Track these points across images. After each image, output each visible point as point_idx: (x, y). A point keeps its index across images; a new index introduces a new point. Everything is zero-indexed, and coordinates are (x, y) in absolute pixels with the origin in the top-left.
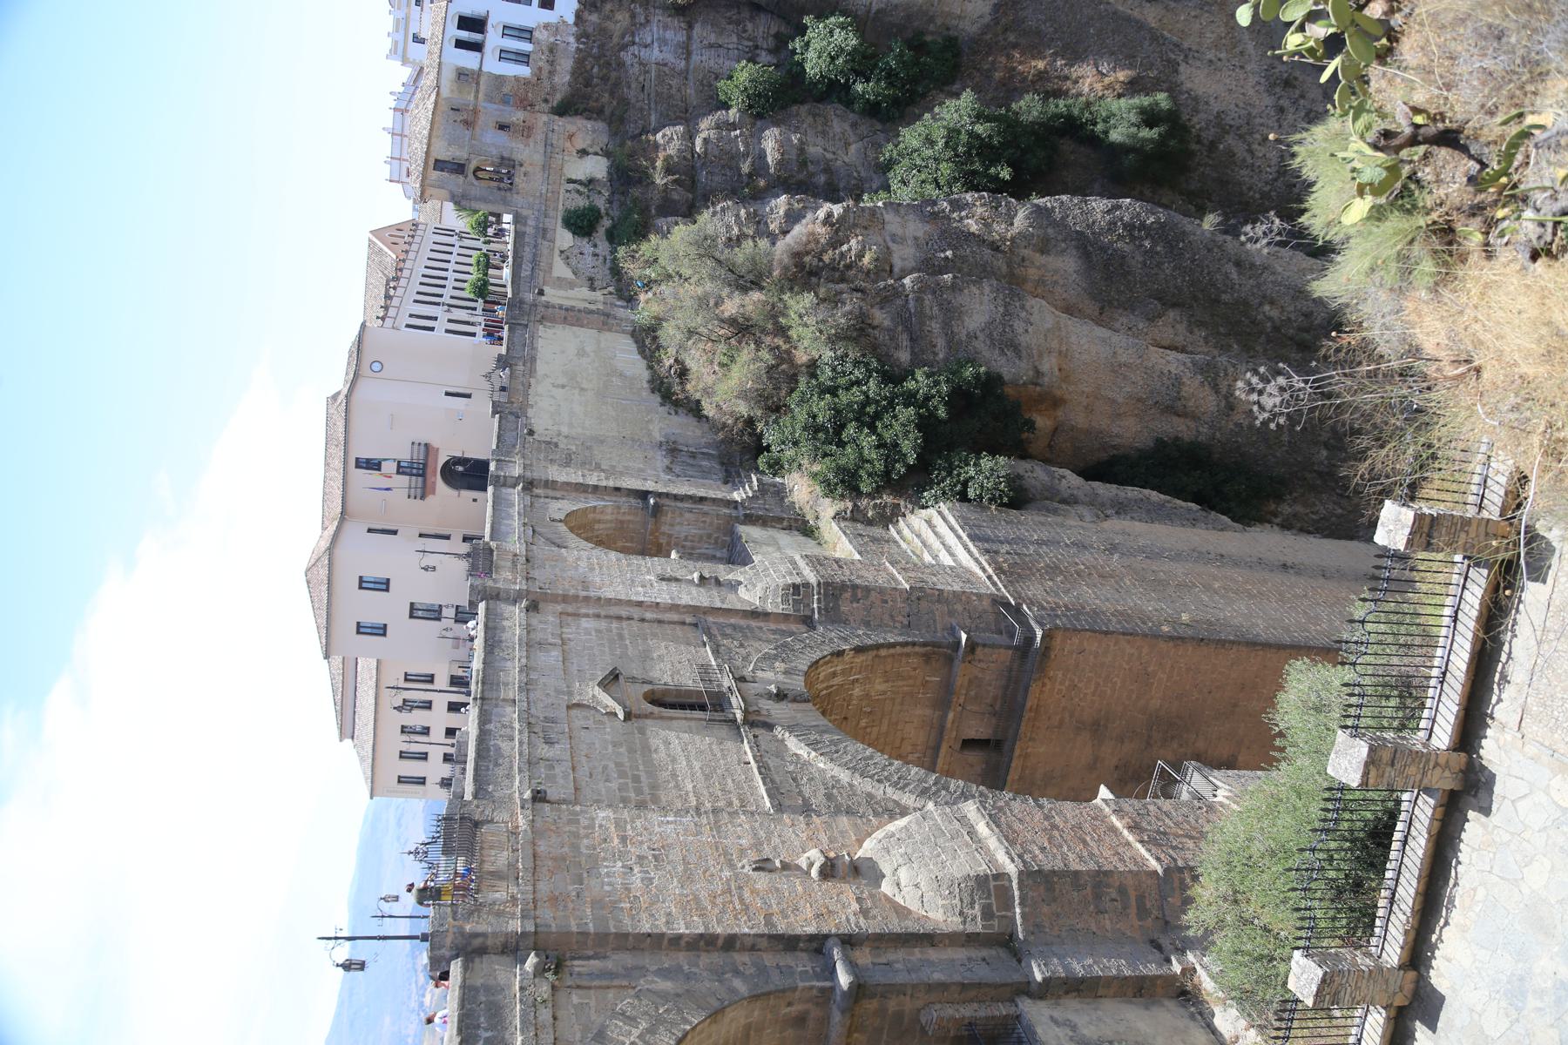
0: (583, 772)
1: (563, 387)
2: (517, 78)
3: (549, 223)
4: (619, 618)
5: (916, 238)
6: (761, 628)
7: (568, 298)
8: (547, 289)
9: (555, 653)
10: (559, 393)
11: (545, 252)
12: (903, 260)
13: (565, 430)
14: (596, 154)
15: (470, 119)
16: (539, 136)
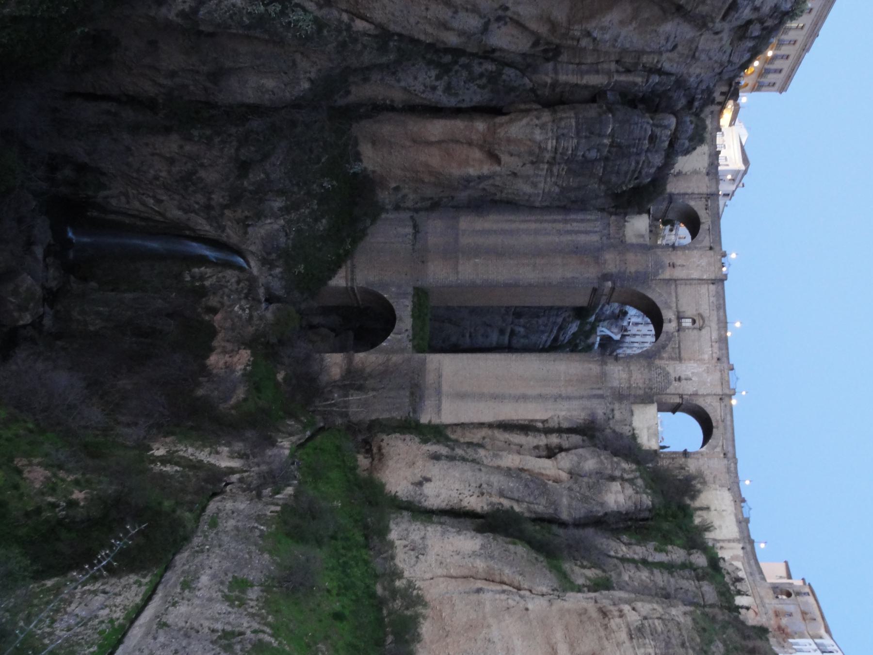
0: (707, 294)
1: (723, 511)
2: (794, 638)
3: (751, 578)
4: (699, 360)
5: (611, 493)
6: (667, 360)
7: (732, 548)
8: (740, 553)
9: (713, 338)
10: (724, 508)
11: (748, 568)
12: (617, 486)
13: (718, 492)
14: (742, 607)
15: (805, 615)
16: (771, 613)
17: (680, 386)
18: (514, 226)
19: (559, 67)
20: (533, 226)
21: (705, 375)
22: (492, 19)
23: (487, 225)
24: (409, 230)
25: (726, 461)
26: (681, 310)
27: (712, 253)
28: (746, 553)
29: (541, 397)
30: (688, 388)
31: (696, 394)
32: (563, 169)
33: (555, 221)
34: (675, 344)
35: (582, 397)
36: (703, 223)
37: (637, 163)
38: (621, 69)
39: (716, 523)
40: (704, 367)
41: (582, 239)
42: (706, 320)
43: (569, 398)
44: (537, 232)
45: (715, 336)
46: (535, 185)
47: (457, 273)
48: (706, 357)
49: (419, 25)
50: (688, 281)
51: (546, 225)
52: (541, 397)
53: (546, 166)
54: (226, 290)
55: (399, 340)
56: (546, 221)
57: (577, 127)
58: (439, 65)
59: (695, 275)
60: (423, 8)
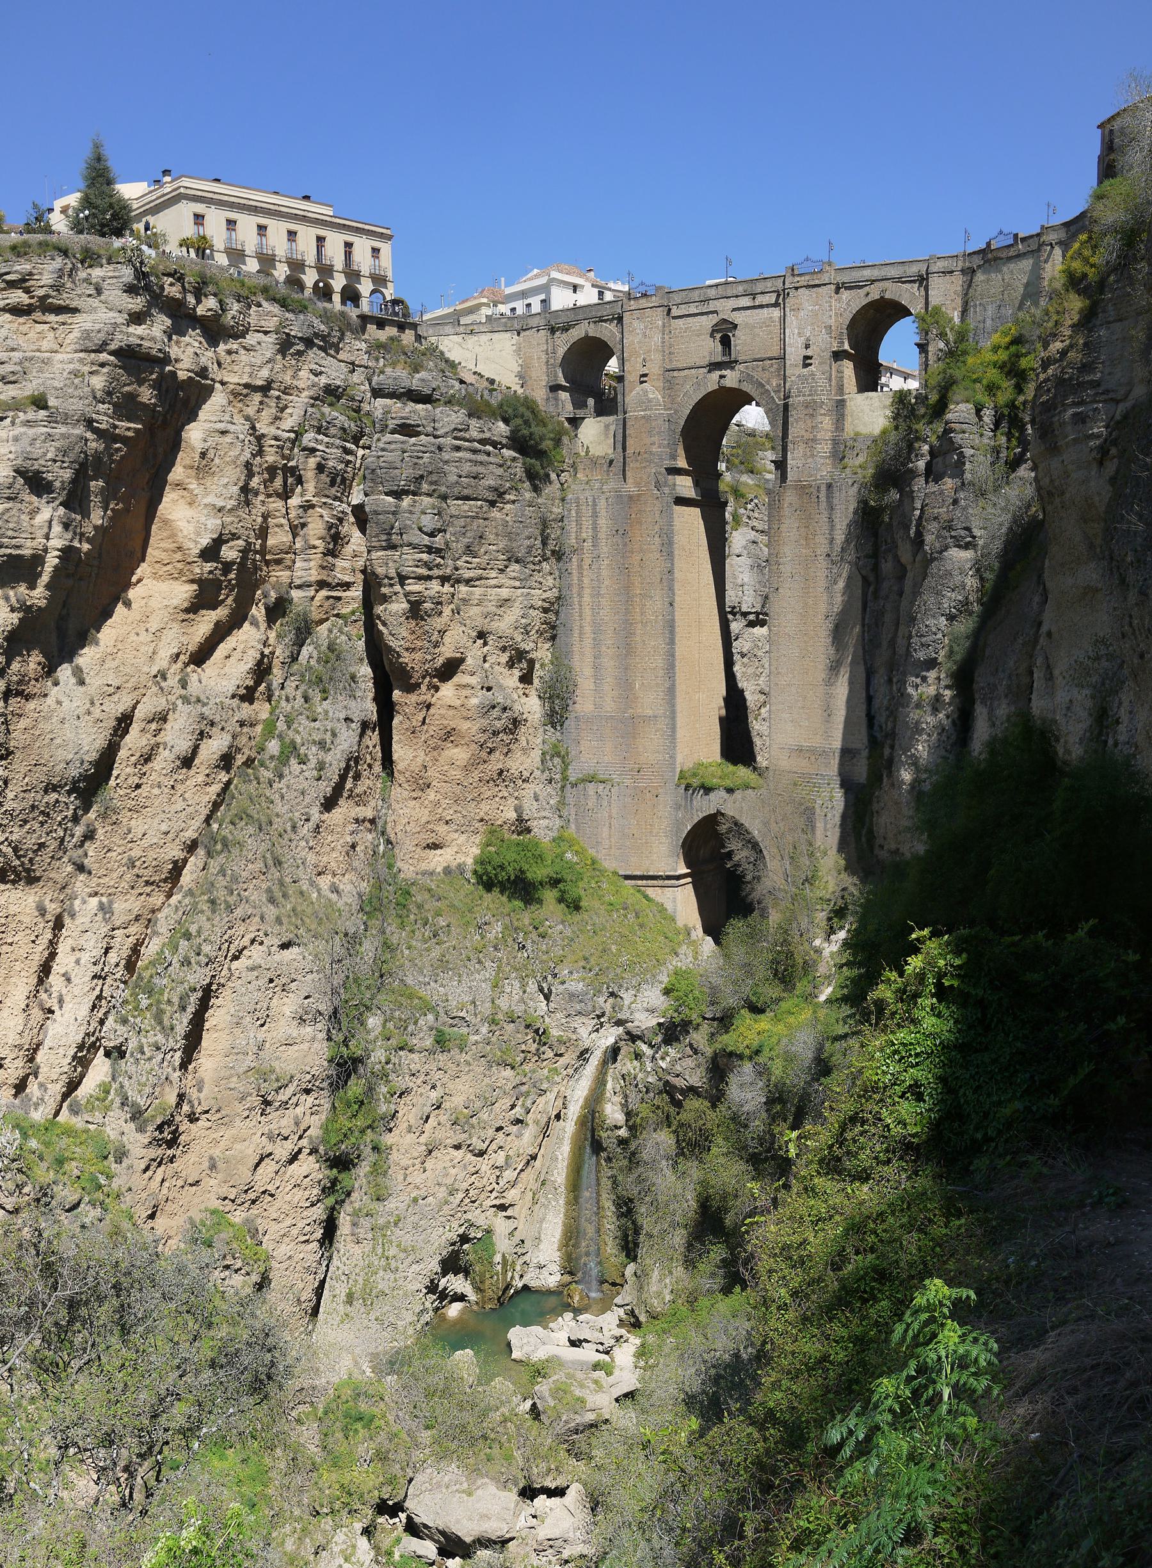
9: (749, 304)
17: (819, 355)
18: (588, 629)
19: (298, 582)
20: (587, 599)
21: (802, 313)
22: (183, 692)
23: (588, 671)
24: (591, 788)
32: (467, 562)
33: (580, 567)
34: (758, 366)
36: (587, 331)
37: (458, 449)
38: (299, 489)
42: (721, 316)
45: (745, 302)
46: (505, 602)
48: (776, 313)
49: (186, 796)
50: (667, 351)
51: (586, 581)
53: (463, 589)
54: (640, 1076)
56: (580, 580)
57: (385, 549)
58: (283, 759)
59: (657, 338)
60: (156, 791)
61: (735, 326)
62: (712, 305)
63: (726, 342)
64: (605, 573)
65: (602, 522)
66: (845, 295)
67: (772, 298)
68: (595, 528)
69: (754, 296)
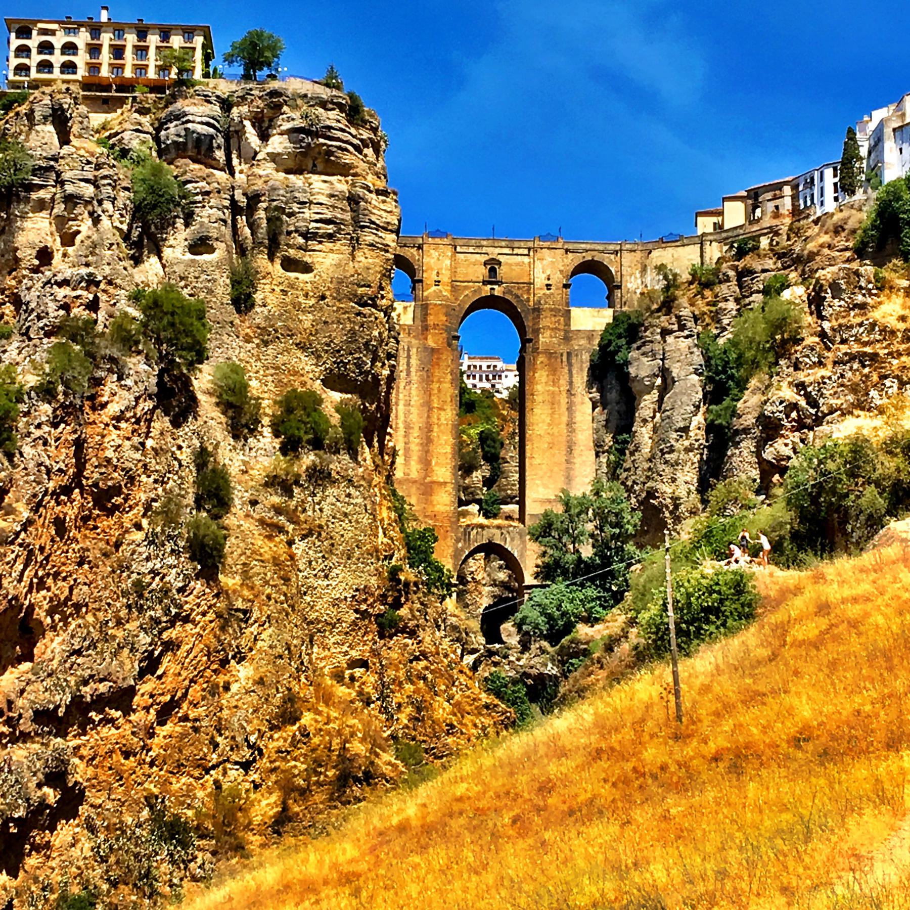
20: (401, 407)
21: (545, 262)
25: (625, 254)
26: (481, 279)
27: (425, 247)
28: (715, 240)
29: (570, 409)
30: (558, 279)
31: (561, 271)
35: (570, 371)
39: (689, 264)
40: (537, 263)
41: (414, 361)
43: (571, 383)
44: (408, 404)
45: (507, 251)
47: (446, 483)
48: (526, 260)
50: (454, 272)
51: (401, 396)
52: (570, 409)
55: (512, 539)
59: (448, 262)
61: (499, 263)
62: (484, 250)
63: (493, 271)
64: (414, 392)
65: (414, 361)
66: (570, 255)
67: (526, 252)
68: (408, 364)
69: (513, 248)
